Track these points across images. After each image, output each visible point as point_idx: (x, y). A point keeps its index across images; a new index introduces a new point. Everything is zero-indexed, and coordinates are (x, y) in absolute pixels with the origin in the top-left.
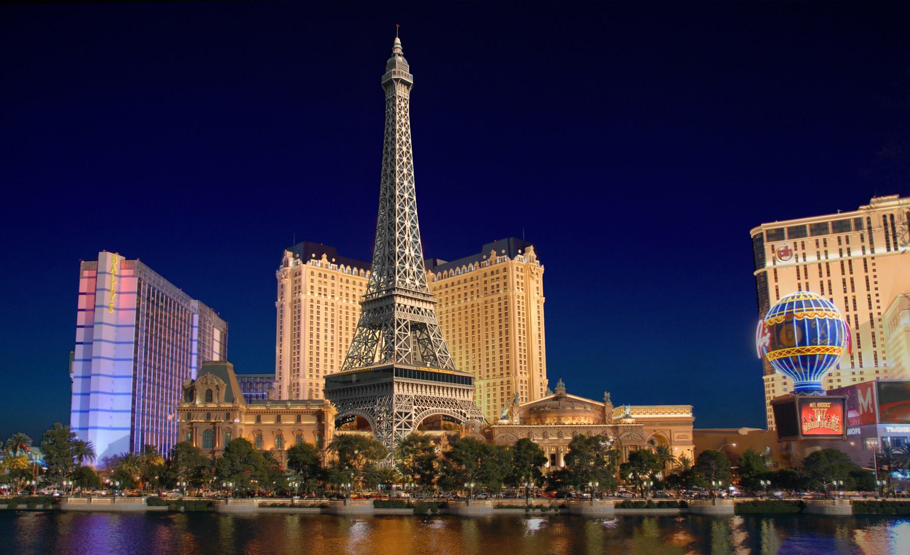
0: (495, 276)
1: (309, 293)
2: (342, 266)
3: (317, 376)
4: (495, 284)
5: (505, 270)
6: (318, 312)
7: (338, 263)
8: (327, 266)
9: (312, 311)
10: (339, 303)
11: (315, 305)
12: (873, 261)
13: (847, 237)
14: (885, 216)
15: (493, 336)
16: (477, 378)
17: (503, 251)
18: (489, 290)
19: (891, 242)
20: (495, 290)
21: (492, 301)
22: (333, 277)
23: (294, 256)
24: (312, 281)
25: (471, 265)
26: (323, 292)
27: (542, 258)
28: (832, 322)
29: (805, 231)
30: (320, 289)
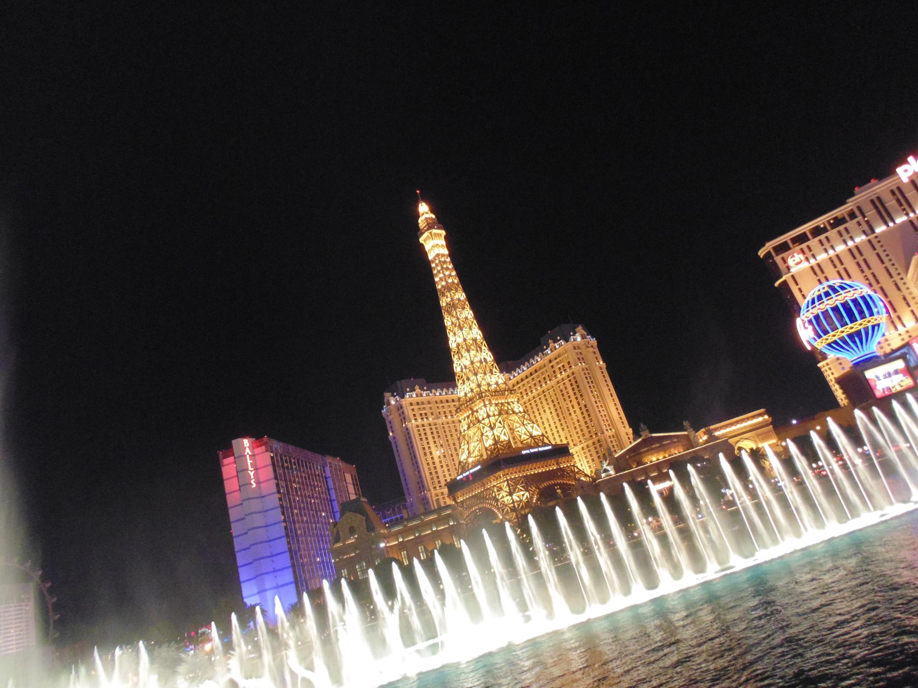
1: (413, 421)
2: (433, 391)
4: (560, 365)
6: (425, 434)
7: (429, 389)
8: (422, 396)
9: (420, 435)
11: (421, 429)
15: (573, 407)
16: (571, 444)
18: (558, 372)
19: (887, 218)
24: (413, 410)
25: (536, 357)
26: (424, 417)
27: (591, 331)
29: (807, 236)
30: (421, 414)
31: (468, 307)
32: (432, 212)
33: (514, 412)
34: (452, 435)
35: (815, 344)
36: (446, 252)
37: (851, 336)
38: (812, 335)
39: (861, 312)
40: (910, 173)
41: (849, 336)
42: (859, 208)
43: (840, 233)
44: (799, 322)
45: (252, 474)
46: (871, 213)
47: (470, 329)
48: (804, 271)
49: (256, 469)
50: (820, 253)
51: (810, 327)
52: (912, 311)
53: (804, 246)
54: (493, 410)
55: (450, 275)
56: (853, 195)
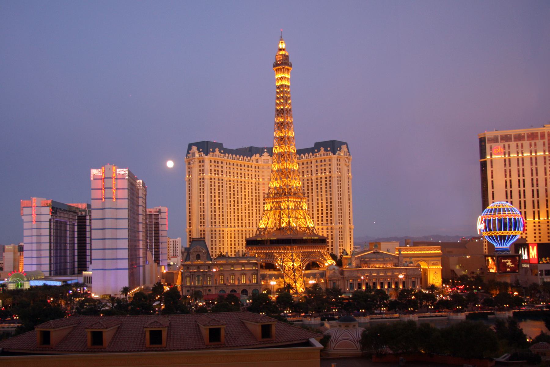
0: (323, 163)
2: (227, 155)
3: (215, 226)
5: (330, 160)
10: (226, 179)
11: (213, 181)
15: (322, 199)
17: (329, 149)
18: (319, 171)
20: (323, 171)
21: (321, 178)
22: (222, 162)
23: (198, 149)
24: (211, 166)
26: (217, 173)
28: (515, 219)
34: (245, 203)
35: (483, 233)
37: (500, 236)
38: (483, 228)
39: (510, 227)
41: (499, 236)
43: (531, 145)
44: (480, 217)
50: (513, 153)
51: (484, 224)
52: (547, 211)
53: (506, 144)
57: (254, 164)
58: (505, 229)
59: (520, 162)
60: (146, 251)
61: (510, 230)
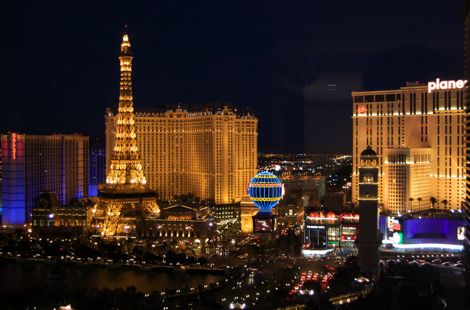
12: (403, 119)
13: (392, 104)
14: (411, 94)
19: (413, 109)
31: (132, 105)
32: (130, 43)
33: (135, 169)
36: (130, 70)
37: (257, 202)
40: (433, 88)
42: (404, 95)
45: (14, 152)
46: (407, 102)
47: (128, 119)
48: (363, 118)
49: (17, 150)
50: (375, 112)
53: (369, 104)
54: (124, 166)
55: (127, 85)
56: (404, 86)
57: (168, 118)
58: (258, 197)
59: (380, 121)
60: (87, 185)
61: (262, 197)
